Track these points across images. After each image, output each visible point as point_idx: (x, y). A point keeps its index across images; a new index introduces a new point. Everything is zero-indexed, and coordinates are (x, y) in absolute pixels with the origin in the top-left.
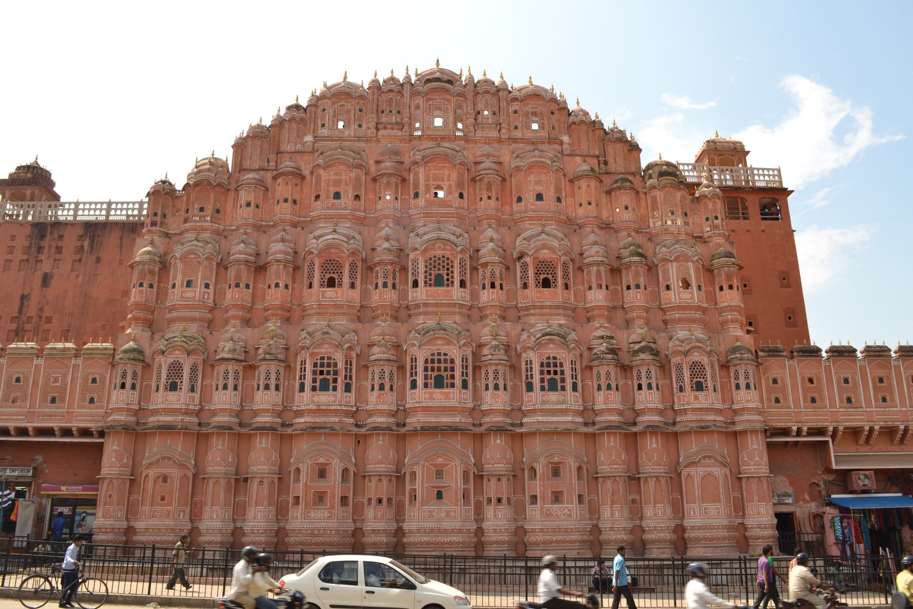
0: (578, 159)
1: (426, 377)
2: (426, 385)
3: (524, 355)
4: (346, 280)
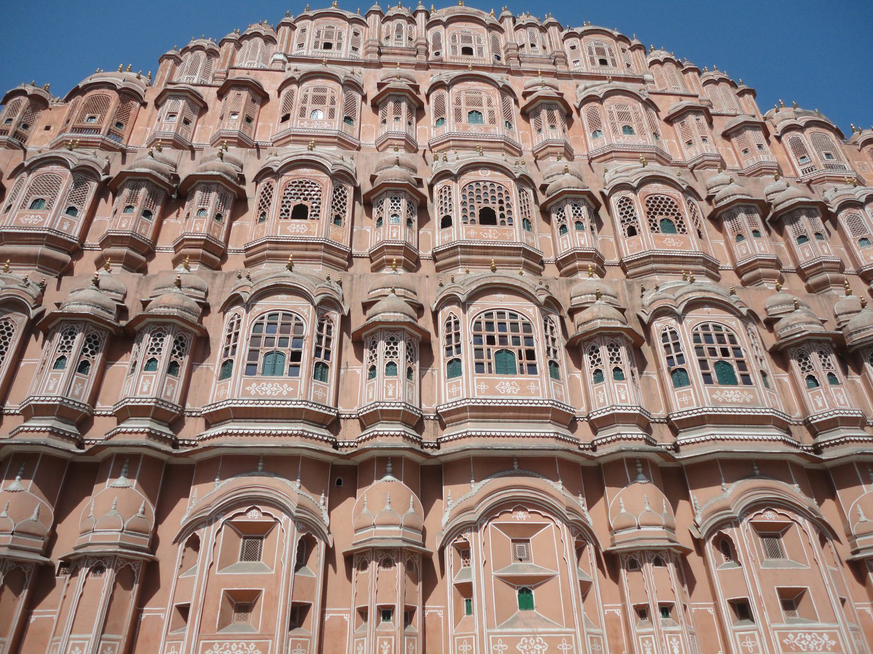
0: (671, 97)
1: (478, 352)
2: (479, 367)
3: (658, 327)
4: (326, 211)
